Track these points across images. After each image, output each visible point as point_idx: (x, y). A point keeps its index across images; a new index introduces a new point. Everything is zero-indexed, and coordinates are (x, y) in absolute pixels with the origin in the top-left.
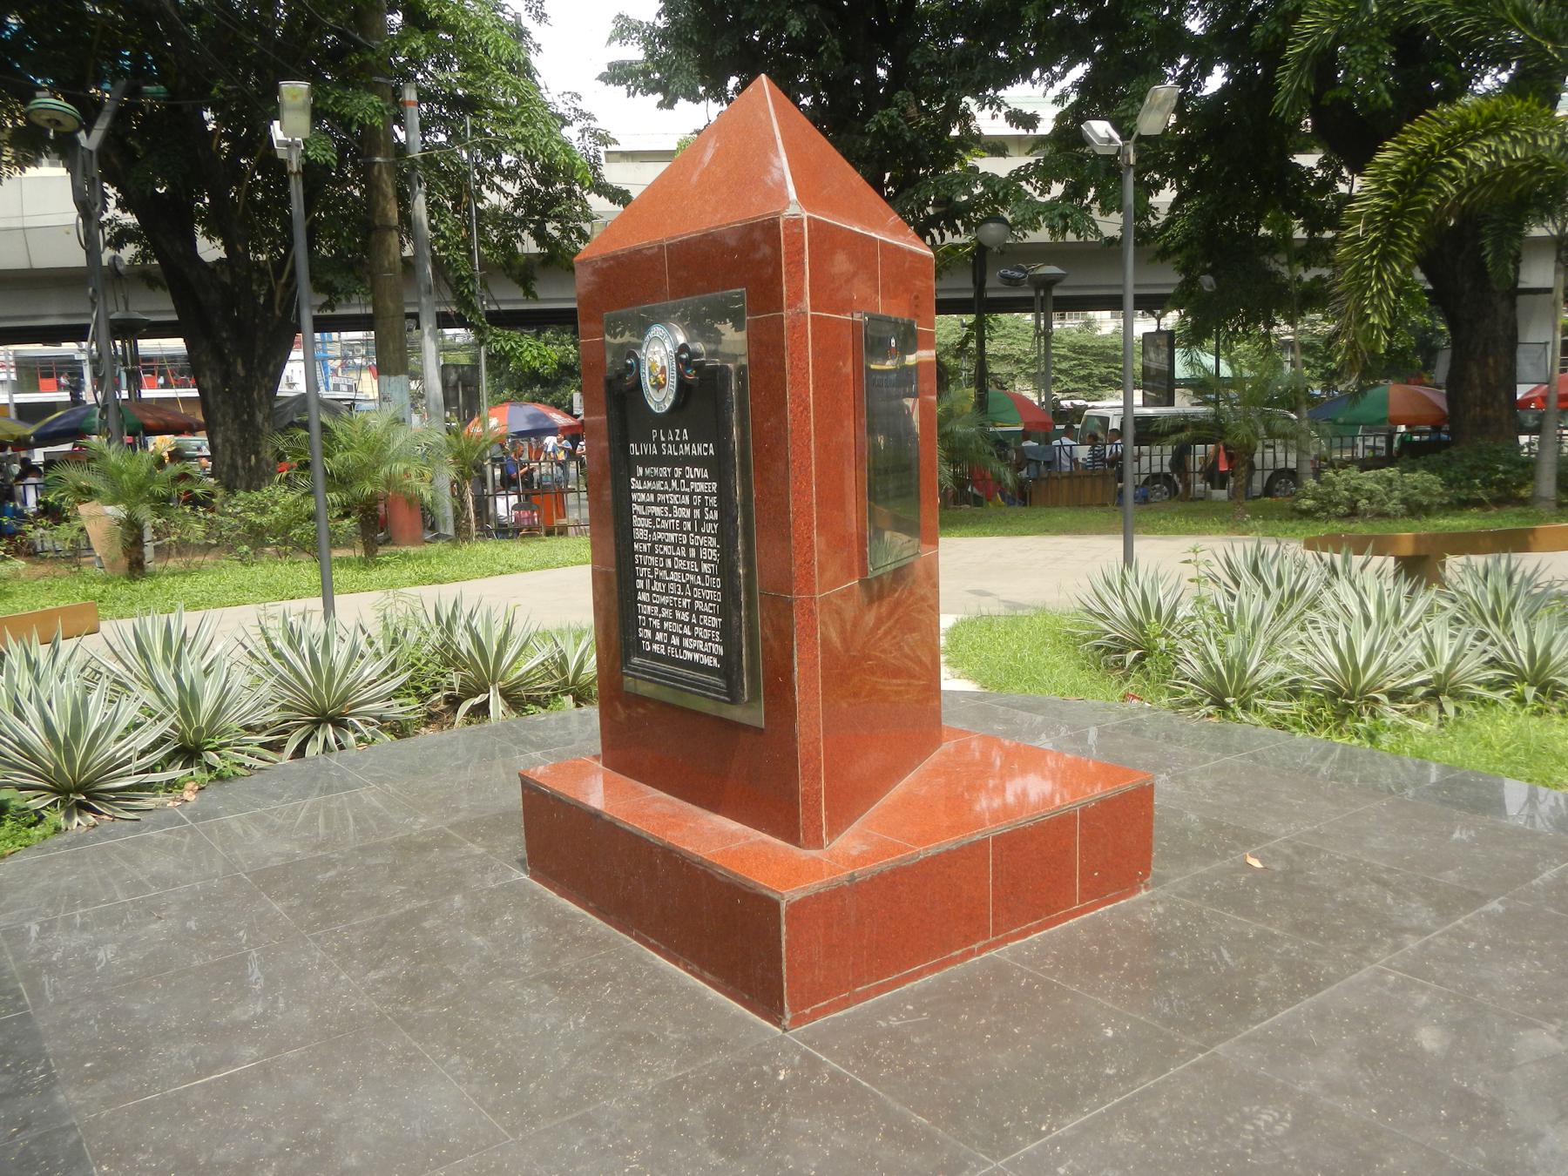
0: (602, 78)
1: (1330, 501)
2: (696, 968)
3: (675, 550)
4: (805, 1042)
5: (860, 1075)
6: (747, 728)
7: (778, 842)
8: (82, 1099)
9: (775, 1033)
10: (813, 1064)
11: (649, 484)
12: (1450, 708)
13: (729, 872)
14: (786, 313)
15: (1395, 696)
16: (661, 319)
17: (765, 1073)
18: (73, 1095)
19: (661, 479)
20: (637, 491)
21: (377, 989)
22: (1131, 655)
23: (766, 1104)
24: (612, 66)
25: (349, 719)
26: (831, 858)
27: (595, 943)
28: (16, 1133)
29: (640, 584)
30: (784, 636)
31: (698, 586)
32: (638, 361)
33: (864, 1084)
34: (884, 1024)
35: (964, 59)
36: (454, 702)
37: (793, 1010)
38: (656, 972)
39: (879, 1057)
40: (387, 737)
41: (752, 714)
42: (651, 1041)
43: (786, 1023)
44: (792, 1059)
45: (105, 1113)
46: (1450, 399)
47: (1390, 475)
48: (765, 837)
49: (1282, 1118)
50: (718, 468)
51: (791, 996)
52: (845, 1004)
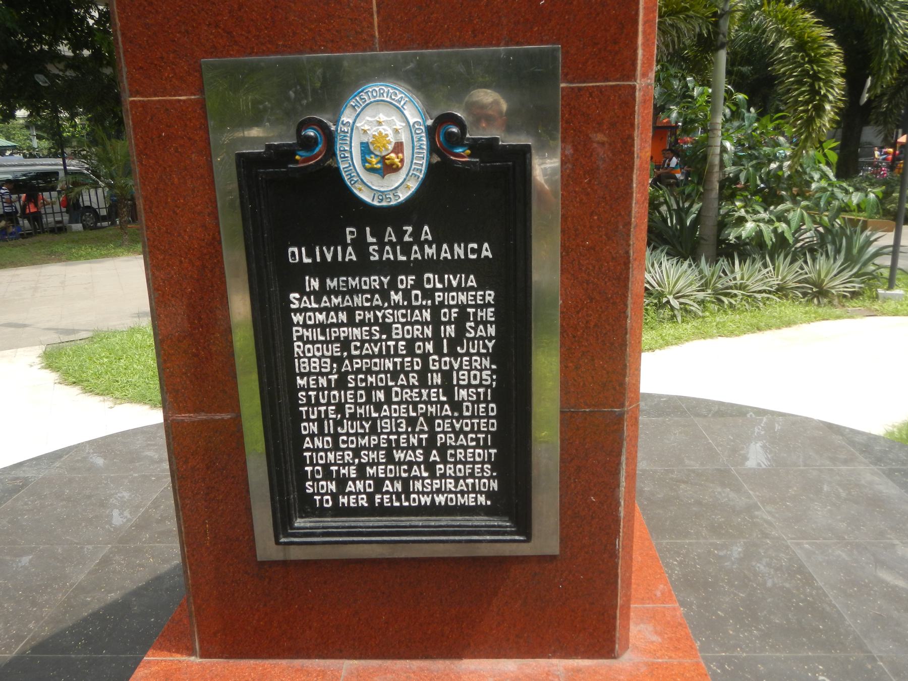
11: (336, 301)
19: (364, 292)
32: (330, 138)
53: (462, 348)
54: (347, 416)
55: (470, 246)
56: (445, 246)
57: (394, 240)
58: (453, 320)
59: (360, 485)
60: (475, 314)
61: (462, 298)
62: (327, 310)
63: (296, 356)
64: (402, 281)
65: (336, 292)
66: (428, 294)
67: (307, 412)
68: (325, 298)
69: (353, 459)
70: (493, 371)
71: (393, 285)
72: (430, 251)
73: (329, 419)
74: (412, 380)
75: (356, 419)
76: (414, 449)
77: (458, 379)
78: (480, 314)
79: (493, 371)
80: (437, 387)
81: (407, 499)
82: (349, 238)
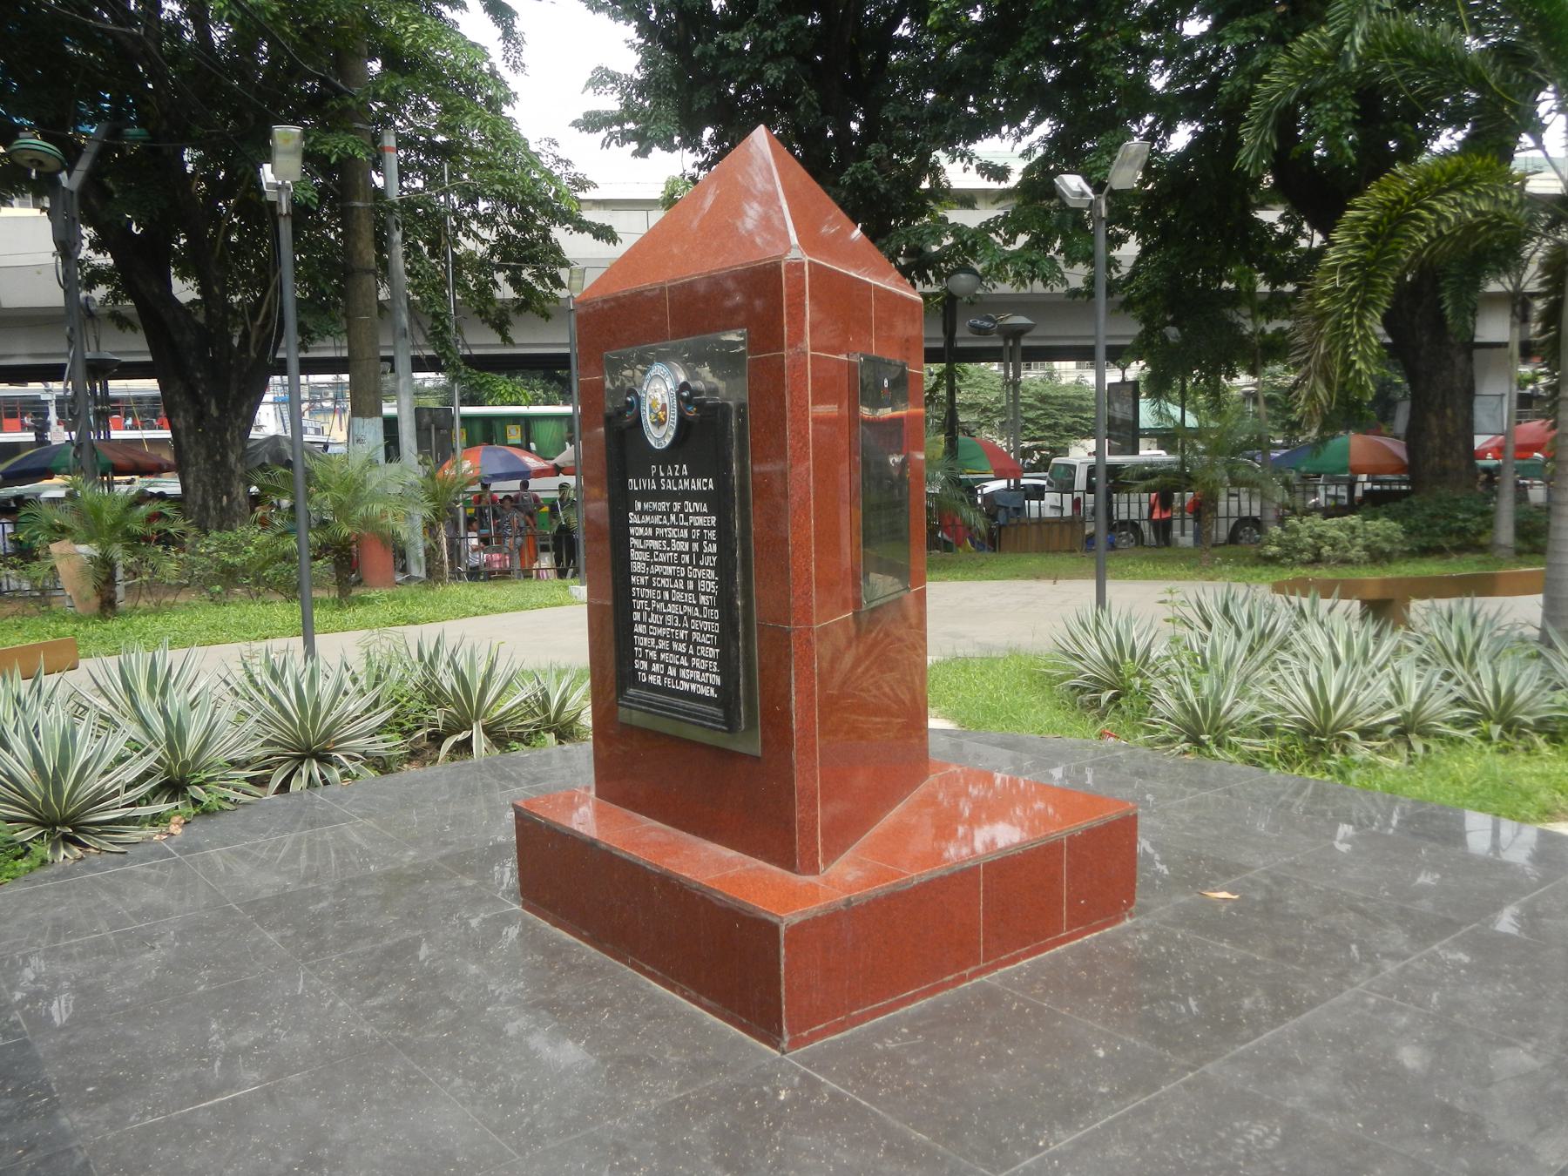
0: (575, 124)
1: (1295, 548)
2: (693, 993)
3: (673, 583)
4: (804, 1064)
5: (860, 1094)
6: (743, 756)
7: (774, 868)
8: (88, 1121)
9: (773, 1055)
10: (812, 1085)
11: (648, 518)
12: (1418, 746)
13: (727, 897)
14: (787, 352)
15: (1366, 733)
16: (662, 358)
17: (765, 1094)
18: (76, 1117)
19: (659, 513)
20: (635, 525)
21: (376, 1015)
22: (1108, 694)
23: (768, 1123)
24: (587, 115)
25: (334, 754)
26: (827, 883)
27: (590, 971)
28: (20, 1157)
29: (637, 616)
30: (782, 663)
31: (696, 618)
32: (638, 399)
33: (864, 1103)
34: (880, 1047)
35: (937, 115)
36: (436, 739)
37: (791, 1032)
38: (652, 998)
39: (877, 1078)
40: (371, 773)
41: (752, 745)
42: (652, 1064)
43: (784, 1045)
44: (792, 1079)
45: (110, 1135)
46: (1410, 450)
47: (1352, 522)
48: (761, 863)
49: (1272, 1132)
50: (718, 502)
51: (789, 1021)
52: (841, 1027)
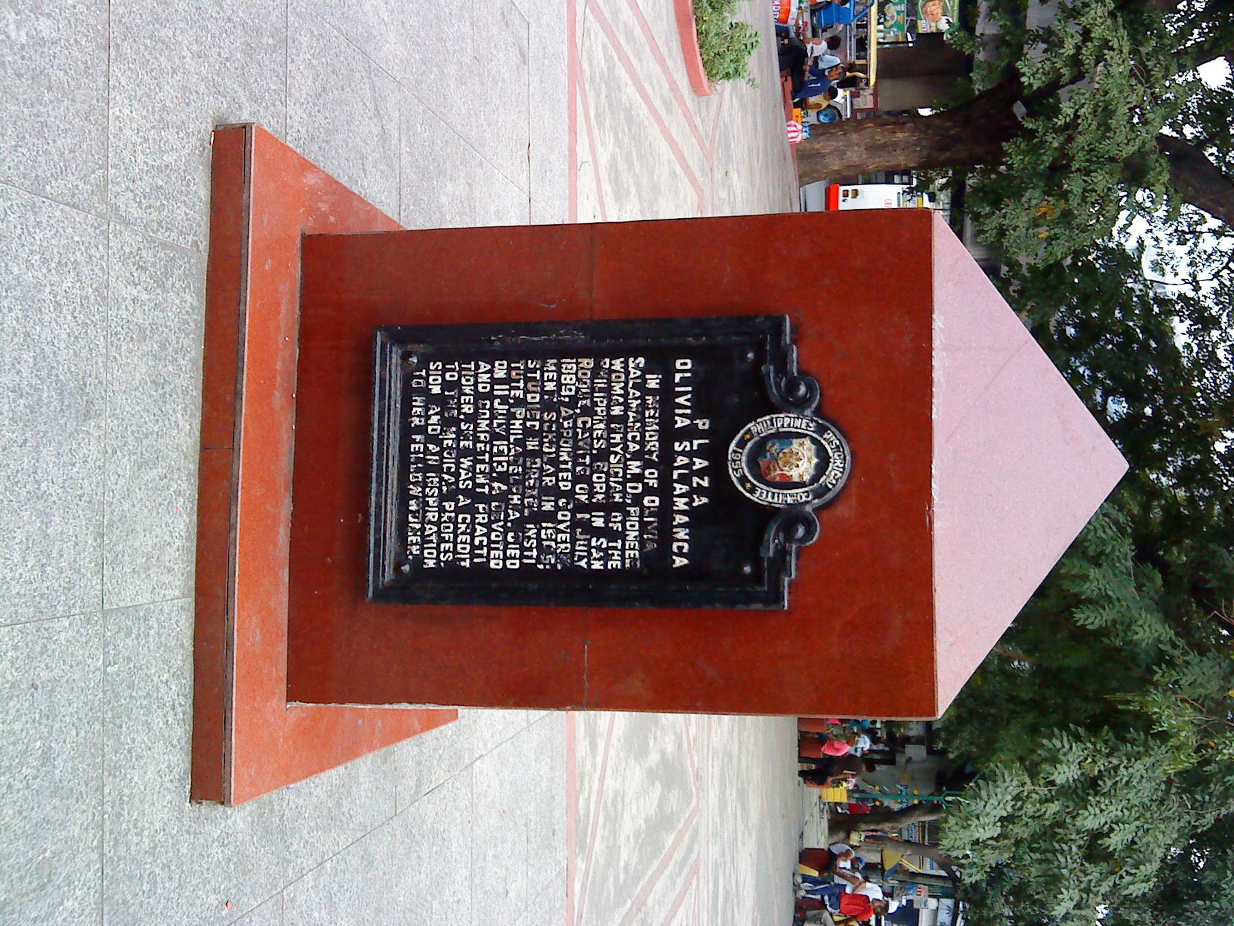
53: (580, 534)
54: (512, 410)
55: (686, 545)
56: (686, 519)
57: (694, 468)
58: (610, 525)
59: (435, 419)
60: (615, 548)
61: (632, 535)
62: (625, 395)
63: (579, 360)
64: (653, 473)
65: (644, 406)
66: (637, 500)
67: (519, 368)
68: (638, 394)
69: (465, 414)
70: (555, 565)
71: (648, 464)
72: (681, 504)
73: (509, 390)
74: (547, 479)
75: (508, 420)
76: (473, 479)
77: (547, 528)
78: (616, 553)
79: (555, 565)
80: (540, 506)
81: (417, 470)
82: (699, 422)
